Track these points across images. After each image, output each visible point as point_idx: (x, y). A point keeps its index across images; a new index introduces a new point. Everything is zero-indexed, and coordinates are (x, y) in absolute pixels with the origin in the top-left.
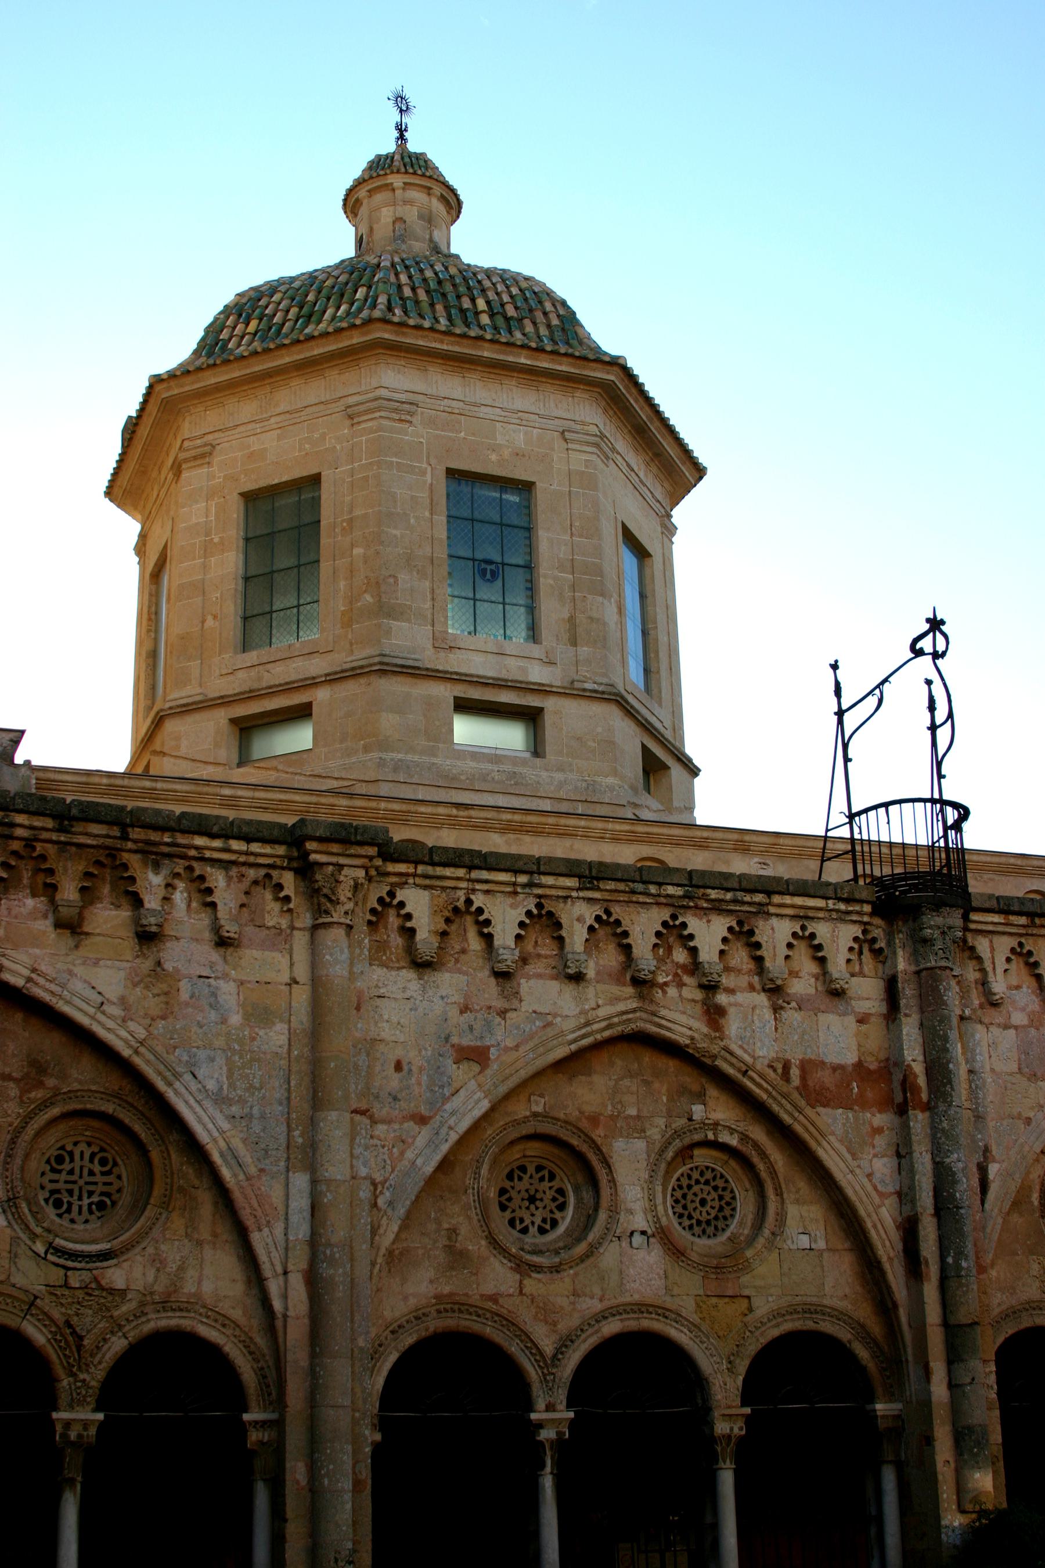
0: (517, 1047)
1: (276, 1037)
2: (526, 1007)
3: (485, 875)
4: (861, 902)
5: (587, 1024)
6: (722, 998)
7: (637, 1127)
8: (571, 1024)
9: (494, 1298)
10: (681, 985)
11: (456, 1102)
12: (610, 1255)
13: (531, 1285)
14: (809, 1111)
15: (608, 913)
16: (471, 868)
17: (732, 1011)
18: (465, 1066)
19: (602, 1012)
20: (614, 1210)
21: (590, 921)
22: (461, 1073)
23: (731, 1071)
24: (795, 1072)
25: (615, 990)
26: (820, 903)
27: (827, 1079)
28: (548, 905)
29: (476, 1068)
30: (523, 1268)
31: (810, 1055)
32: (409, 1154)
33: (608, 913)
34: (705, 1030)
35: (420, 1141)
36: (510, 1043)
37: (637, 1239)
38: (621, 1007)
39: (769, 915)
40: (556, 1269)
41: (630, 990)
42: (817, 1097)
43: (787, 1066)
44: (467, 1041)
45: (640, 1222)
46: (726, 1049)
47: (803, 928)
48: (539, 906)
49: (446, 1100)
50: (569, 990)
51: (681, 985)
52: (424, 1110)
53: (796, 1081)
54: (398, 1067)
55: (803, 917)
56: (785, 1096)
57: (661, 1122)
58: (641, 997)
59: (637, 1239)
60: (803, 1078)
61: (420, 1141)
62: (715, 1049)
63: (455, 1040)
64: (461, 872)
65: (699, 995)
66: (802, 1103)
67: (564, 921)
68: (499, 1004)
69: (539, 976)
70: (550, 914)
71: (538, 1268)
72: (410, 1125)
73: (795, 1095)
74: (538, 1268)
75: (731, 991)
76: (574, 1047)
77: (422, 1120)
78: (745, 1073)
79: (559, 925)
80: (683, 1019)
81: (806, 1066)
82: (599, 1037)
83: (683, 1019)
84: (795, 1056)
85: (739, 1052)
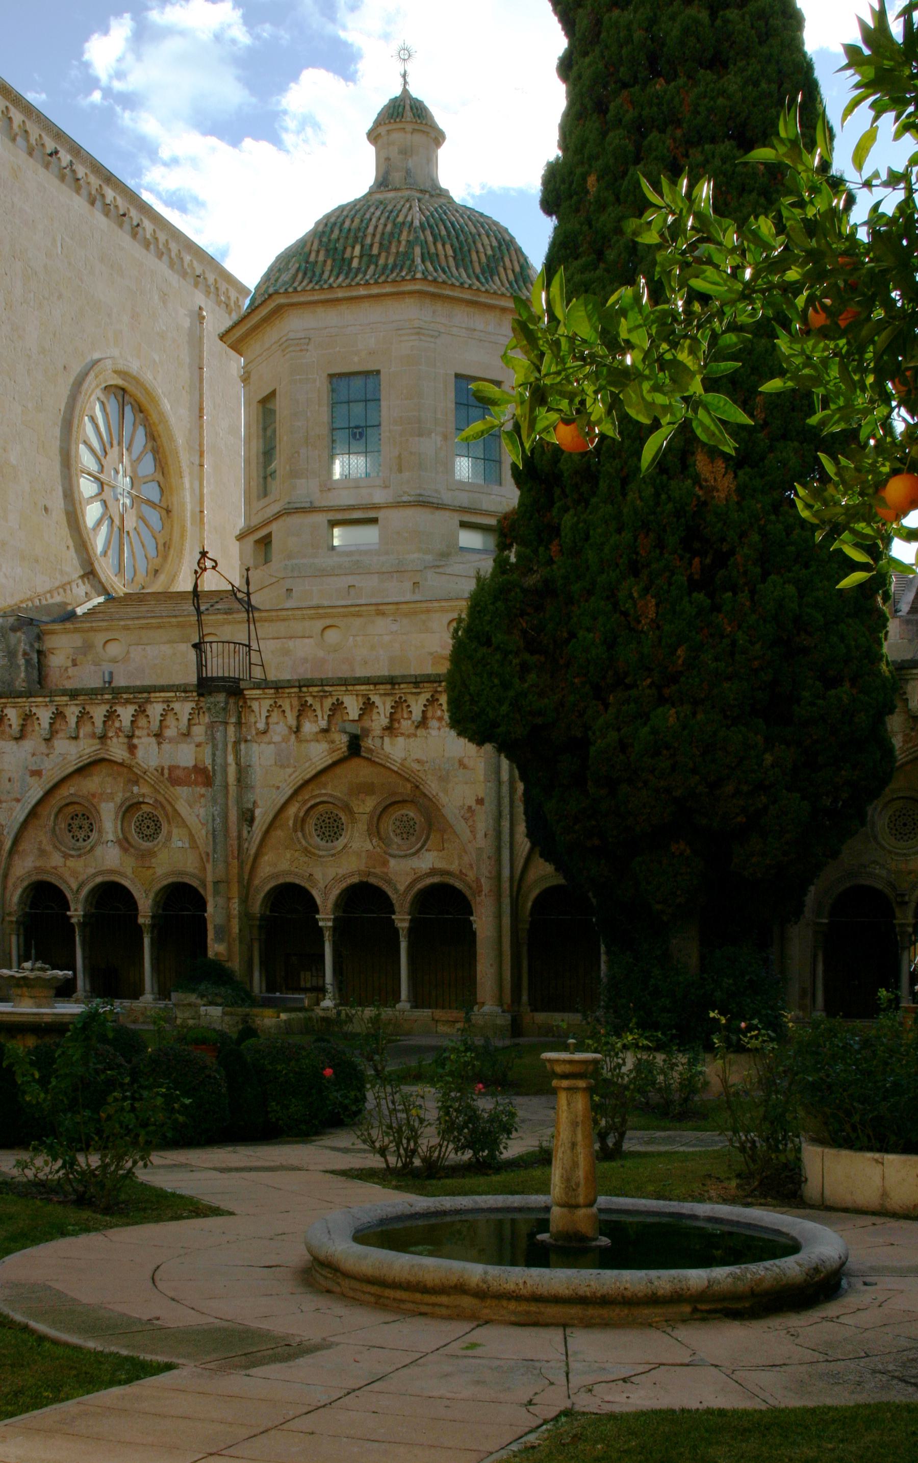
0: (52, 769)
2: (57, 752)
3: (33, 699)
4: (192, 691)
5: (81, 757)
6: (135, 741)
8: (74, 757)
9: (55, 868)
10: (118, 737)
11: (31, 792)
16: (28, 697)
17: (140, 746)
18: (34, 778)
19: (87, 751)
20: (100, 832)
21: (77, 713)
22: (32, 781)
23: (139, 772)
24: (166, 772)
25: (91, 741)
26: (172, 694)
27: (179, 773)
28: (61, 709)
29: (38, 778)
30: (66, 856)
31: (173, 763)
32: (14, 814)
34: (128, 755)
35: (18, 809)
36: (50, 767)
38: (94, 748)
39: (152, 702)
40: (80, 856)
41: (97, 741)
42: (175, 781)
43: (163, 769)
44: (34, 768)
46: (137, 763)
47: (168, 706)
48: (57, 709)
49: (27, 792)
50: (74, 742)
51: (118, 737)
52: (19, 796)
53: (166, 775)
55: (167, 701)
58: (102, 743)
60: (170, 774)
61: (18, 809)
62: (133, 763)
63: (30, 768)
64: (24, 700)
65: (126, 740)
66: (169, 784)
67: (67, 714)
68: (45, 751)
69: (61, 738)
70: (61, 712)
71: (72, 856)
72: (14, 803)
73: (166, 782)
74: (72, 856)
75: (139, 737)
76: (75, 767)
77: (18, 800)
79: (65, 717)
81: (172, 769)
82: (86, 762)
83: (119, 752)
84: (166, 764)
85: (142, 764)
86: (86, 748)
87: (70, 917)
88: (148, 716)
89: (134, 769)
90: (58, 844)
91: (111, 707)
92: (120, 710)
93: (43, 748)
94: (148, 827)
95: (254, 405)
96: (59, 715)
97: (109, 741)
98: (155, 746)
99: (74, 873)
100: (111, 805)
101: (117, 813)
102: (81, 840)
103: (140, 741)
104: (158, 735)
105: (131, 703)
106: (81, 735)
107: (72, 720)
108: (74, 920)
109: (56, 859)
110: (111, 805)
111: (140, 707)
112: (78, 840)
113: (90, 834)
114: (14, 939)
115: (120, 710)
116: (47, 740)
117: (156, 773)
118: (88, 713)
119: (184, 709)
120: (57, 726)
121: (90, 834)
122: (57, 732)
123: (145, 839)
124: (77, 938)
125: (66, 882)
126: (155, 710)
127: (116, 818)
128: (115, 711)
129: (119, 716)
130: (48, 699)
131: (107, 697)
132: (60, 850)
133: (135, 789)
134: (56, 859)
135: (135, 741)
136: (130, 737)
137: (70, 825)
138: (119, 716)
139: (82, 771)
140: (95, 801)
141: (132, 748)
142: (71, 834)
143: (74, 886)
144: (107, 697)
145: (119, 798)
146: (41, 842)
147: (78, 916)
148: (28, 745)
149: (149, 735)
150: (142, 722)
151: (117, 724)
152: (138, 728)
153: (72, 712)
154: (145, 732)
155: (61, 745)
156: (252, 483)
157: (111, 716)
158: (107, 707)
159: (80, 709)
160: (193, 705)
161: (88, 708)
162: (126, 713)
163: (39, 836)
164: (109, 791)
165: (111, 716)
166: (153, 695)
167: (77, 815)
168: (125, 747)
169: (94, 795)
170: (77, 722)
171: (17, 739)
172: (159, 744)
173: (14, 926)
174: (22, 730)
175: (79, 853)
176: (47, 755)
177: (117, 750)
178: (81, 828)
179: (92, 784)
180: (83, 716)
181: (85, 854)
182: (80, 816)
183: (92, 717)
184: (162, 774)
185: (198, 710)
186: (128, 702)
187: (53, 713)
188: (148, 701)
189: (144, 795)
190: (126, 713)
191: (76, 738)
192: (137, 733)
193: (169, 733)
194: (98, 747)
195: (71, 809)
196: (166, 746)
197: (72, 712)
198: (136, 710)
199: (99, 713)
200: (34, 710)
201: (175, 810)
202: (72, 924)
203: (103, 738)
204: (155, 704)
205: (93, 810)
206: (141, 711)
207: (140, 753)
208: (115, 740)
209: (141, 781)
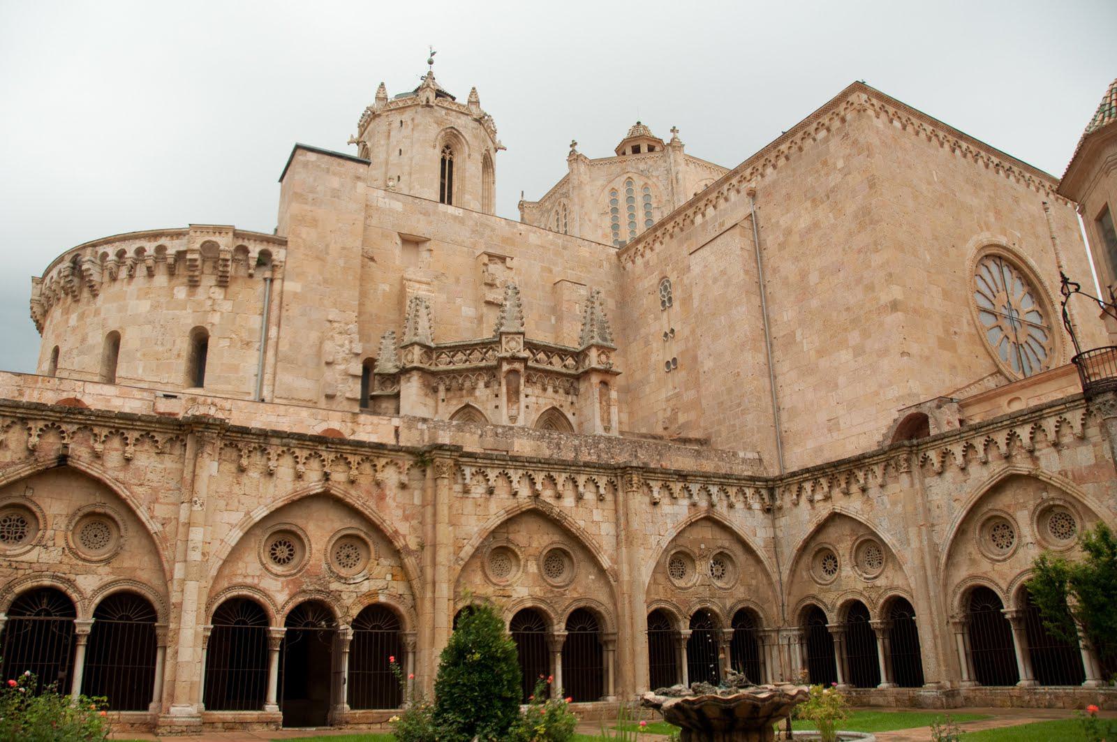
1: (899, 508)
7: (1024, 506)
8: (987, 478)
9: (985, 573)
12: (1021, 552)
13: (998, 566)
14: (1077, 487)
15: (989, 437)
19: (996, 471)
20: (1020, 537)
21: (983, 442)
22: (955, 504)
23: (1045, 479)
25: (999, 462)
28: (970, 442)
32: (945, 533)
33: (989, 437)
37: (1030, 545)
40: (1004, 560)
41: (1004, 461)
45: (1029, 539)
48: (967, 443)
54: (938, 507)
56: (1068, 484)
57: (1032, 502)
58: (1008, 462)
59: (1030, 545)
62: (1038, 473)
66: (1074, 485)
67: (975, 445)
71: (998, 561)
73: (1071, 482)
74: (998, 561)
78: (1050, 479)
80: (1024, 465)
83: (1024, 465)
86: (997, 469)
87: (1004, 614)
88: (1044, 430)
89: (1040, 477)
90: (986, 554)
91: (1011, 431)
92: (1018, 431)
93: (961, 477)
94: (1063, 526)
95: (1093, 223)
96: (969, 447)
97: (1014, 460)
98: (1056, 455)
99: (1002, 576)
100: (1026, 512)
101: (1032, 519)
102: (1004, 546)
103: (1041, 453)
104: (1056, 445)
105: (1027, 423)
106: (990, 459)
107: (980, 448)
108: (1008, 616)
109: (985, 566)
110: (1026, 512)
111: (1035, 425)
112: (1002, 547)
113: (1011, 540)
114: (960, 637)
115: (1018, 431)
116: (963, 469)
117: (1061, 477)
118: (993, 440)
119: (1075, 417)
120: (970, 456)
121: (1011, 540)
122: (970, 462)
123: (1062, 537)
124: (1013, 632)
125: (997, 585)
126: (1050, 424)
127: (1032, 524)
128: (1015, 433)
129: (1018, 436)
130: (958, 437)
131: (1005, 423)
132: (987, 557)
133: (1045, 495)
134: (985, 566)
135: (1037, 454)
136: (1031, 452)
137: (993, 536)
138: (1018, 436)
139: (997, 488)
140: (1011, 511)
141: (1035, 460)
142: (996, 543)
143: (1004, 587)
144: (1005, 423)
145: (1031, 505)
146: (970, 553)
147: (1012, 612)
148: (949, 475)
149: (1048, 446)
150: (1040, 436)
151: (1018, 443)
152: (1037, 442)
153: (979, 443)
154: (1044, 445)
155: (975, 470)
156: (1104, 275)
157: (1012, 437)
158: (1008, 431)
159: (985, 438)
160: (1083, 411)
161: (991, 436)
162: (1024, 433)
163: (971, 547)
164: (1021, 501)
165: (1012, 437)
166: (1044, 412)
167: (998, 527)
168: (1029, 460)
169: (1009, 507)
170: (985, 450)
171: (940, 474)
172: (1059, 451)
173: (959, 627)
174: (942, 466)
175: (1003, 557)
176: (965, 481)
177: (1023, 465)
178: (1003, 536)
179: (1005, 501)
180: (989, 444)
181: (1009, 558)
182: (1001, 527)
183: (996, 443)
184: (1066, 476)
185: (1088, 413)
186: (1024, 422)
187: (965, 447)
188: (1041, 417)
189: (1053, 499)
190: (1024, 433)
191: (985, 463)
192: (1037, 446)
193: (1067, 440)
194: (1006, 465)
195: (992, 523)
196: (1065, 452)
197: (979, 443)
198: (1032, 428)
199: (1001, 438)
200: (949, 447)
201: (1083, 505)
202: (1007, 620)
203: (1008, 457)
204: (1049, 419)
205: (1011, 520)
206: (1037, 428)
207: (1043, 463)
208: (1019, 457)
209: (1049, 487)
